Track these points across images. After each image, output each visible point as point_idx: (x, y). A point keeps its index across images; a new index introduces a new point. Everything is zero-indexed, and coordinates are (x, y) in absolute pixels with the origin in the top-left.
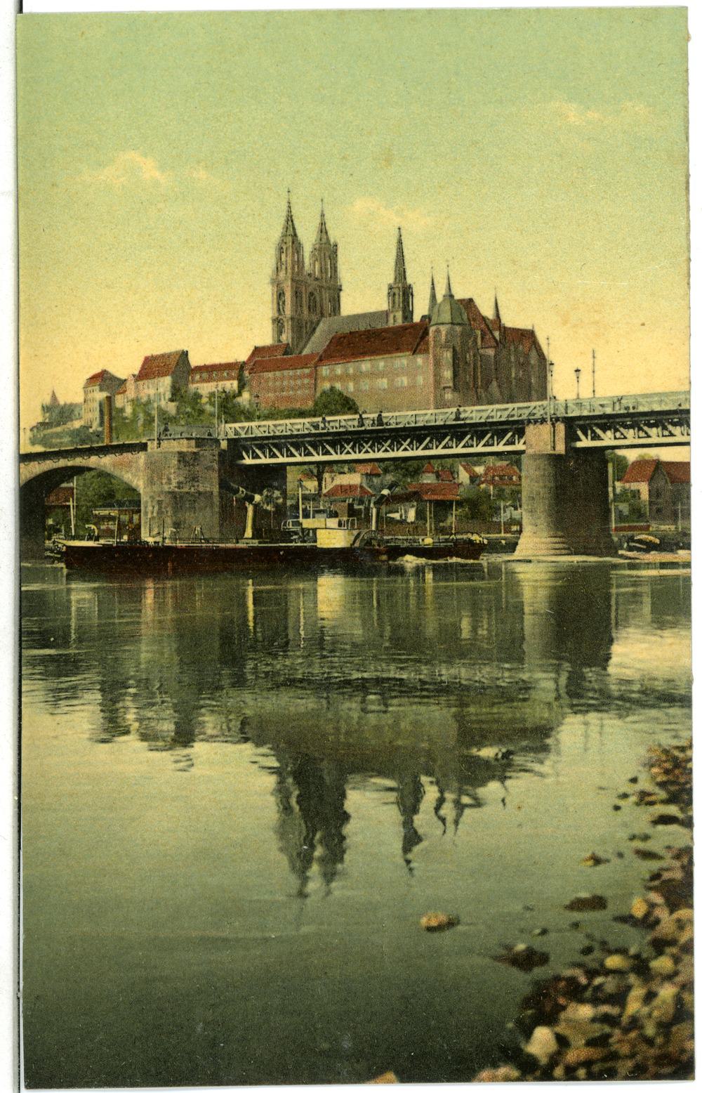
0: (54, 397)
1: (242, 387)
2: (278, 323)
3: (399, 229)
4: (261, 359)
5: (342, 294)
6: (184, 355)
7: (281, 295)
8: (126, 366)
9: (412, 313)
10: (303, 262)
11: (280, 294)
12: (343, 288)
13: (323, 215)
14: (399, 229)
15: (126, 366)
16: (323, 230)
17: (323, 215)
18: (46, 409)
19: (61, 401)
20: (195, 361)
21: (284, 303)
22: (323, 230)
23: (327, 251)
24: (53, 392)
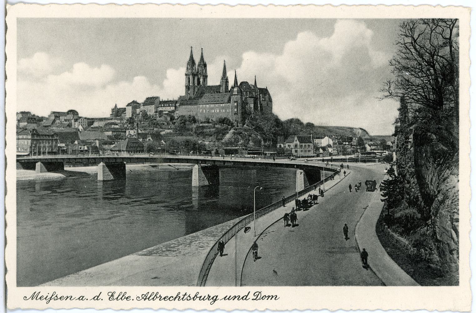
0: (116, 106)
2: (188, 88)
4: (183, 101)
7: (189, 78)
8: (141, 100)
9: (228, 87)
10: (195, 69)
13: (202, 53)
14: (224, 61)
15: (141, 100)
16: (202, 59)
17: (202, 53)
18: (113, 110)
19: (119, 107)
22: (202, 59)
23: (204, 65)
24: (116, 105)
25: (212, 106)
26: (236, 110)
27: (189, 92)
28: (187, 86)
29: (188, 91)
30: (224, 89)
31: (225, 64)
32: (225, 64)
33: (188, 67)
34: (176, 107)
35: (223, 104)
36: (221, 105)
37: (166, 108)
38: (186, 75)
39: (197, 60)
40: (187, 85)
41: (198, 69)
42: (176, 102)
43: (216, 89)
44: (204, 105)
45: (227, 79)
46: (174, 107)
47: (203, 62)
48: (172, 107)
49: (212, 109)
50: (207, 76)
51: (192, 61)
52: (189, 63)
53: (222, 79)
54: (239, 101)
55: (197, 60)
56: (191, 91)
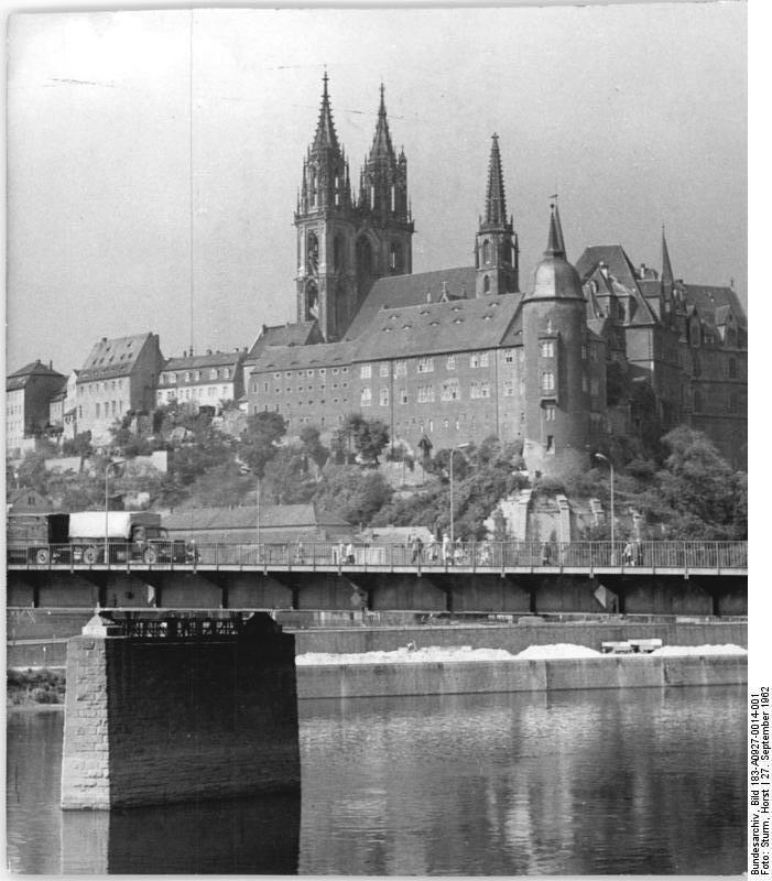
1: (239, 392)
3: (495, 138)
5: (414, 236)
6: (153, 342)
7: (313, 241)
10: (348, 190)
11: (310, 239)
12: (416, 228)
13: (382, 113)
14: (495, 138)
17: (382, 113)
20: (168, 351)
21: (316, 255)
25: (428, 367)
26: (549, 383)
27: (316, 307)
28: (305, 279)
29: (310, 304)
30: (494, 284)
31: (496, 153)
32: (496, 153)
33: (309, 182)
34: (238, 381)
35: (485, 357)
36: (474, 358)
37: (190, 388)
38: (298, 219)
39: (357, 151)
40: (302, 275)
41: (362, 191)
42: (244, 358)
43: (456, 287)
44: (384, 368)
45: (509, 230)
46: (231, 386)
47: (391, 152)
48: (220, 387)
49: (426, 382)
50: (411, 229)
51: (327, 156)
52: (312, 158)
53: (480, 234)
54: (567, 335)
55: (357, 151)
56: (324, 300)
